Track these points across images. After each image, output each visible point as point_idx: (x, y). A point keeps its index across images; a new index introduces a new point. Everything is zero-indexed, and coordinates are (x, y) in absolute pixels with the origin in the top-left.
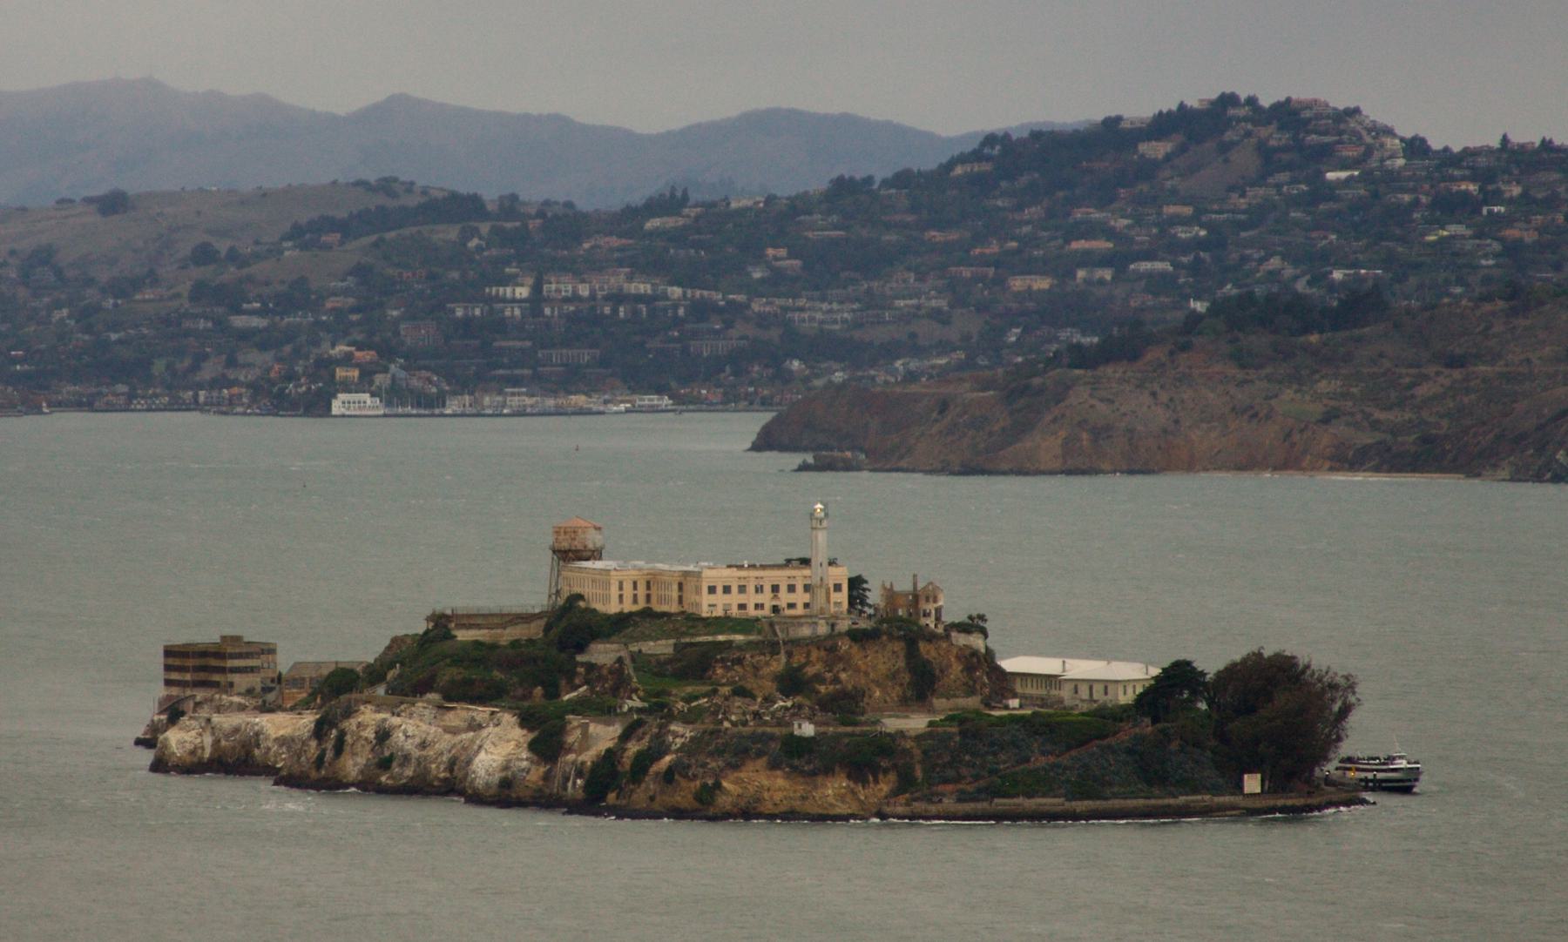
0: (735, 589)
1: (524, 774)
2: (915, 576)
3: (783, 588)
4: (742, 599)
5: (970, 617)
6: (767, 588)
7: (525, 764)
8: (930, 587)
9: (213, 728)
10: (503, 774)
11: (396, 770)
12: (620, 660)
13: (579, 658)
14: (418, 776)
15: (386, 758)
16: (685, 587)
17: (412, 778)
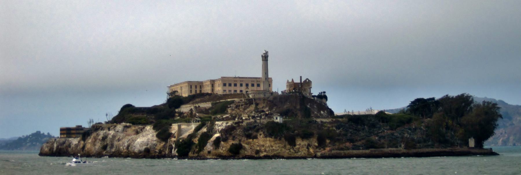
0: (233, 85)
1: (155, 146)
2: (301, 77)
3: (250, 85)
4: (235, 88)
5: (320, 93)
6: (244, 85)
7: (155, 142)
8: (307, 81)
9: (57, 142)
10: (145, 147)
11: (108, 149)
12: (191, 110)
13: (177, 110)
14: (116, 152)
15: (105, 145)
16: (214, 86)
17: (114, 152)
